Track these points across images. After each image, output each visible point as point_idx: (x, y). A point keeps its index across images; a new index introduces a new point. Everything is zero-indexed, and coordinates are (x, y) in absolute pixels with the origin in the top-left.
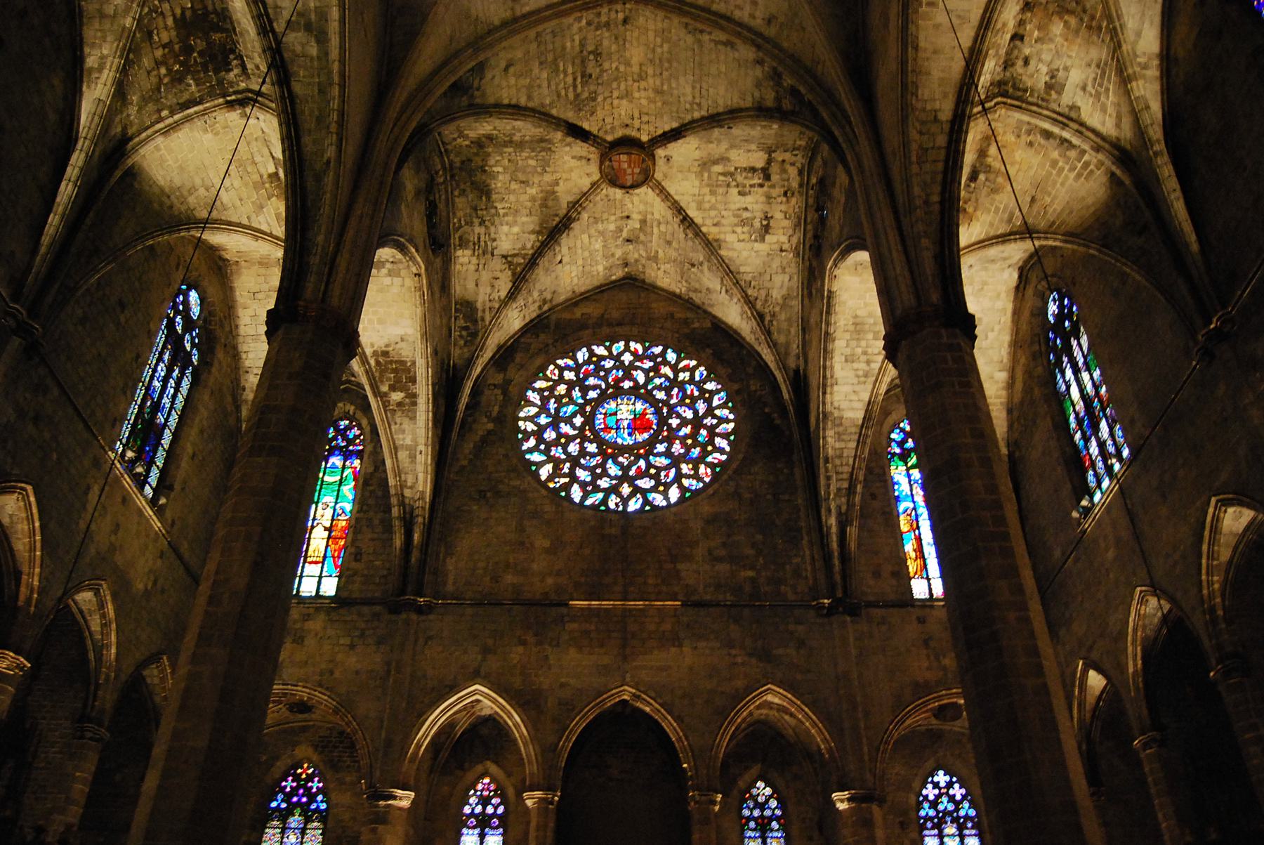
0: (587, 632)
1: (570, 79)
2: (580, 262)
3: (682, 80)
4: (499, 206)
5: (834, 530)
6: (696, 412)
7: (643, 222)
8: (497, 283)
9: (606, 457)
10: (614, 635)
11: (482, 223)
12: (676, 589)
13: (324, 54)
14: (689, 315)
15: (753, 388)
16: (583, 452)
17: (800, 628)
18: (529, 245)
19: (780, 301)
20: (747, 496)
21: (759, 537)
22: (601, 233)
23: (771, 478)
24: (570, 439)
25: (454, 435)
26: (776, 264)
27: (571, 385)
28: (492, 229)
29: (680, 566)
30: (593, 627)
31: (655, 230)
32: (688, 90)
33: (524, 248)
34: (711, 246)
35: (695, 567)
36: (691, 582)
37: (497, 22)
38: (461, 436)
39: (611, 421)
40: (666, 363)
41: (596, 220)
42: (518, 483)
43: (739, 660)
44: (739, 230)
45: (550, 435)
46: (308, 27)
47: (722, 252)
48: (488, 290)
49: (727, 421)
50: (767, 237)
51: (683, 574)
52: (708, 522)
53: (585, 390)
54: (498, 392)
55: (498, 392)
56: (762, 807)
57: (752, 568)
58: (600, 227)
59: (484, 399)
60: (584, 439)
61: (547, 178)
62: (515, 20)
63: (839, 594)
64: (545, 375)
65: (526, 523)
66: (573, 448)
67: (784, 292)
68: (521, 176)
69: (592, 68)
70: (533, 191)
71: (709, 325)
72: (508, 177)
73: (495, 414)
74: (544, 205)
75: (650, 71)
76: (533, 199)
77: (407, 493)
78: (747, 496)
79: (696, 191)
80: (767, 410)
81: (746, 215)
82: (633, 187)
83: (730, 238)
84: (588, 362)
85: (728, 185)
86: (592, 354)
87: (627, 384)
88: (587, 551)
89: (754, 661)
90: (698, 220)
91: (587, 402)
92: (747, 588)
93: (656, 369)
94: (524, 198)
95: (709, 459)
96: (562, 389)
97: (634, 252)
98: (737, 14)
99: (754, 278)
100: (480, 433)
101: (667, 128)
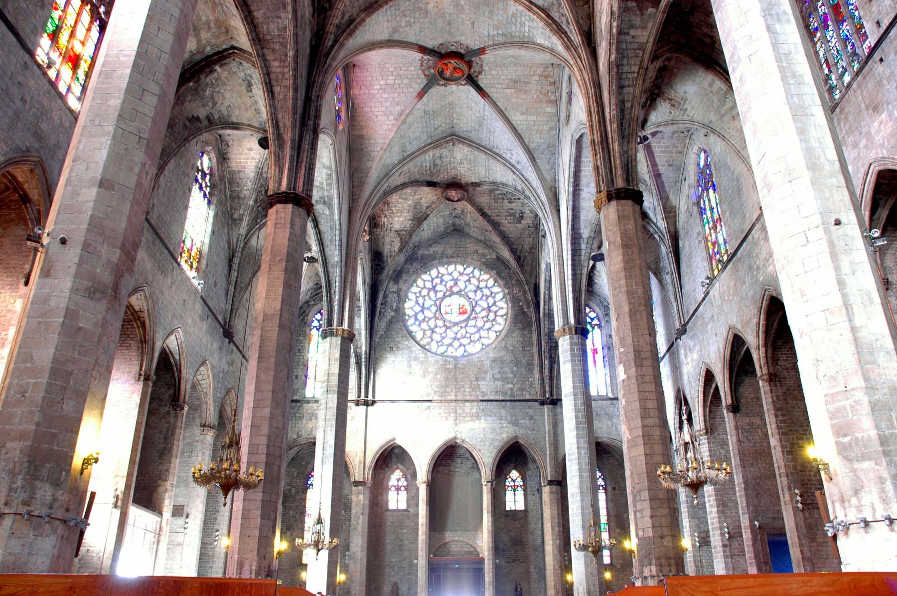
0: (440, 413)
1: (428, 168)
2: (432, 228)
3: (480, 168)
4: (393, 209)
5: (547, 367)
6: (488, 304)
7: (463, 211)
8: (393, 243)
9: (448, 328)
10: (451, 415)
11: (385, 216)
12: (478, 393)
13: (332, 214)
14: (486, 251)
15: (515, 292)
16: (436, 326)
17: (531, 411)
18: (408, 226)
19: (528, 250)
20: (510, 348)
21: (515, 368)
22: (443, 216)
23: (522, 339)
24: (430, 319)
25: (376, 320)
26: (526, 233)
27: (430, 290)
28: (390, 219)
29: (479, 383)
30: (442, 411)
31: (469, 215)
32: (483, 172)
33: (406, 227)
34: (496, 225)
35: (486, 383)
36: (484, 390)
37: (396, 162)
38: (380, 319)
39: (448, 310)
40: (474, 277)
41: (440, 212)
42: (407, 343)
43: (504, 425)
44: (509, 218)
45: (420, 317)
46: (324, 203)
47: (502, 228)
48: (389, 247)
49: (502, 308)
50: (522, 221)
51: (481, 387)
52: (492, 361)
53: (436, 292)
54: (396, 295)
55: (396, 295)
56: (514, 481)
57: (512, 383)
58: (442, 214)
59: (389, 299)
60: (436, 318)
61: (416, 197)
62: (404, 159)
63: (548, 396)
64: (417, 285)
65: (412, 363)
66: (432, 323)
67: (530, 246)
68: (404, 196)
69: (438, 162)
70: (410, 202)
71: (494, 257)
72: (397, 197)
73: (394, 308)
74: (415, 208)
75: (465, 162)
76: (410, 206)
77: (358, 350)
78: (510, 348)
79: (488, 201)
80: (521, 304)
81: (512, 211)
82: (457, 201)
83: (505, 222)
84: (437, 277)
85: (503, 199)
86: (439, 273)
87: (455, 289)
88: (439, 376)
89: (511, 425)
90: (490, 214)
91: (437, 299)
92: (509, 392)
93: (469, 280)
94: (405, 205)
95: (492, 329)
96: (425, 292)
97: (458, 221)
98: (504, 155)
99: (516, 240)
100: (388, 317)
101: (474, 181)
